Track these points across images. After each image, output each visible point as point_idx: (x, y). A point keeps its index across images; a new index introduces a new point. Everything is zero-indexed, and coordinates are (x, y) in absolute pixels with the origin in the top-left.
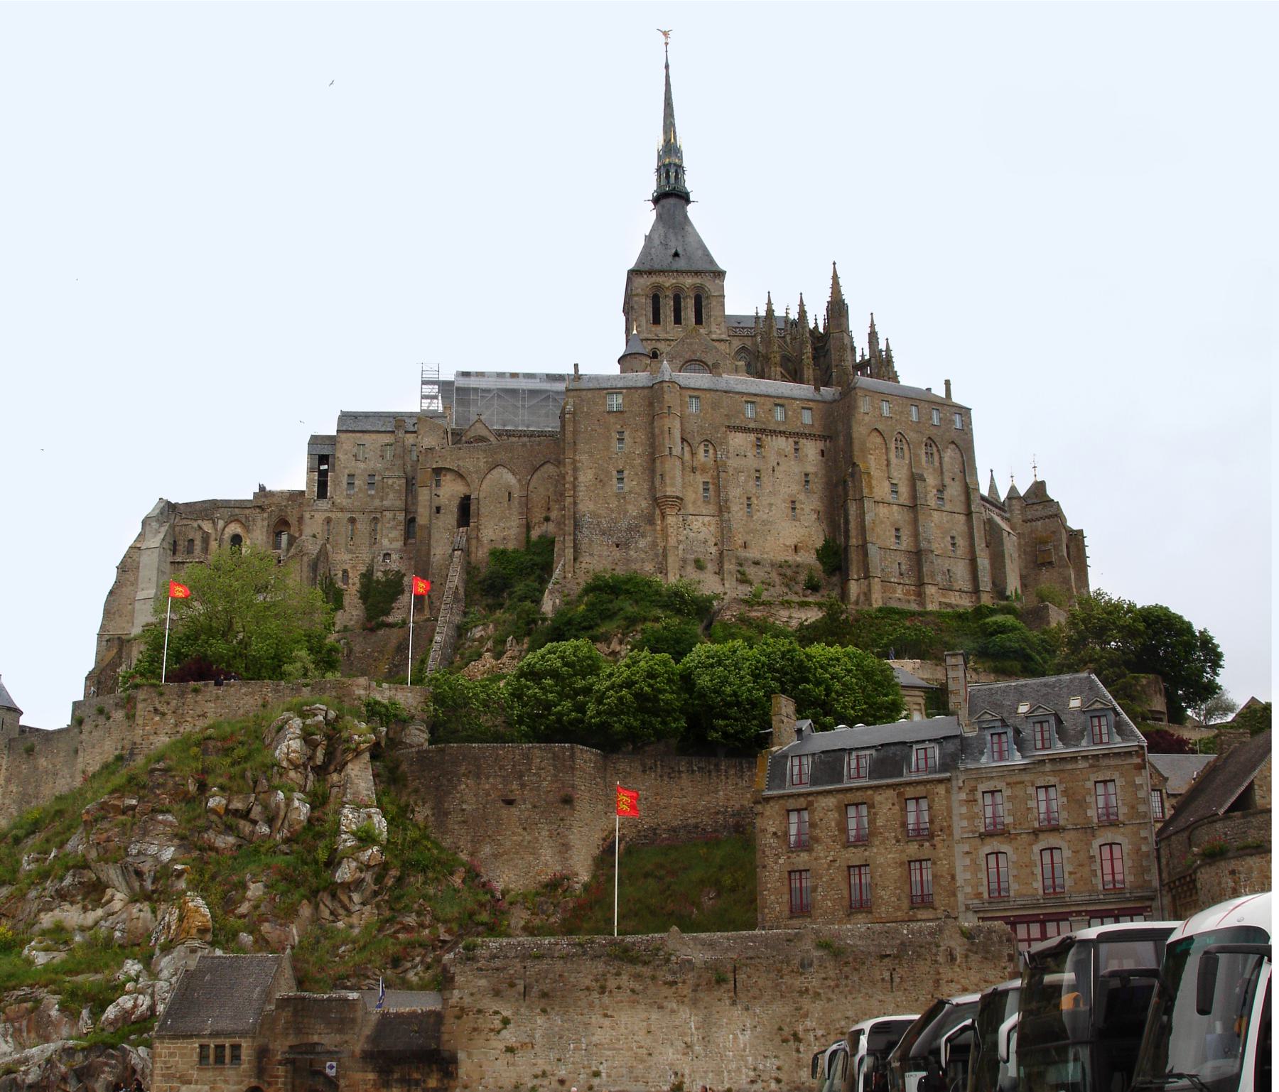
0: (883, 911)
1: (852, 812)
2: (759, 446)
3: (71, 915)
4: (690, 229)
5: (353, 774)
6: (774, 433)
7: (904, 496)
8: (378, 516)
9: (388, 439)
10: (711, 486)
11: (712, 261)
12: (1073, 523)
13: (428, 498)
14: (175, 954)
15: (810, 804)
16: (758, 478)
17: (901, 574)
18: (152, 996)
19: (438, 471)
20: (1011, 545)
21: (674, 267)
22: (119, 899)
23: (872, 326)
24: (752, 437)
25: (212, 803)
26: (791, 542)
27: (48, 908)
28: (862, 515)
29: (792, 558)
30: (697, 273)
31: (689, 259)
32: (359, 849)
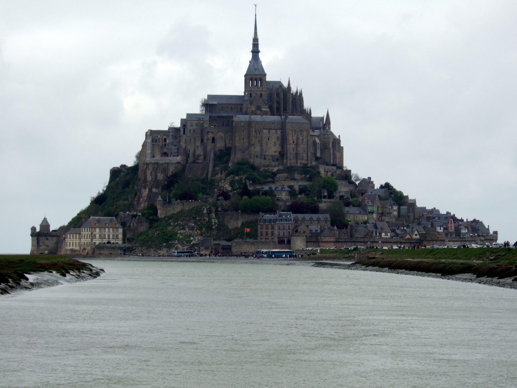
0: (269, 236)
3: (182, 231)
4: (259, 61)
6: (272, 129)
10: (260, 141)
17: (294, 158)
19: (208, 132)
20: (318, 146)
21: (255, 73)
22: (187, 230)
23: (297, 90)
24: (268, 130)
25: (197, 219)
26: (274, 150)
27: (179, 230)
28: (287, 147)
29: (274, 154)
30: (260, 75)
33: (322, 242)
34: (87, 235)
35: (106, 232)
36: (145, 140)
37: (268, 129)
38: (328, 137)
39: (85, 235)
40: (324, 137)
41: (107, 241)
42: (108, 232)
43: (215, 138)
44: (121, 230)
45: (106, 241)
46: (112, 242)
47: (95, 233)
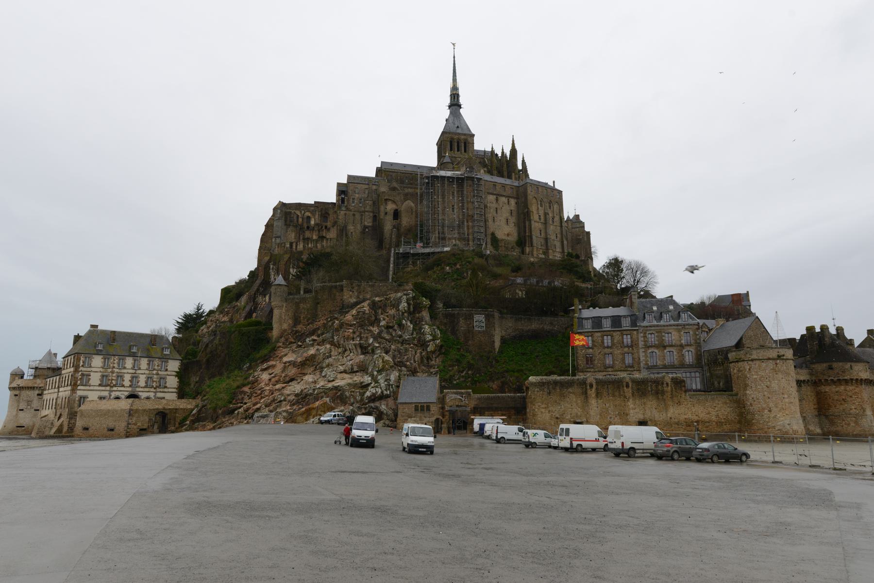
1: (605, 337)
2: (497, 200)
5: (424, 315)
7: (542, 220)
8: (363, 214)
9: (366, 186)
11: (470, 131)
12: (587, 229)
13: (383, 209)
14: (384, 375)
15: (593, 335)
16: (497, 211)
17: (541, 246)
18: (381, 388)
19: (386, 200)
23: (523, 158)
24: (495, 197)
26: (506, 233)
30: (465, 135)
31: (462, 129)
32: (433, 340)
33: (839, 382)
34: (69, 376)
35: (125, 368)
36: (272, 216)
37: (495, 194)
38: (582, 225)
39: (66, 377)
40: (574, 226)
41: (127, 394)
42: (133, 368)
43: (399, 210)
44: (174, 366)
45: (123, 392)
46: (143, 395)
47: (89, 369)
